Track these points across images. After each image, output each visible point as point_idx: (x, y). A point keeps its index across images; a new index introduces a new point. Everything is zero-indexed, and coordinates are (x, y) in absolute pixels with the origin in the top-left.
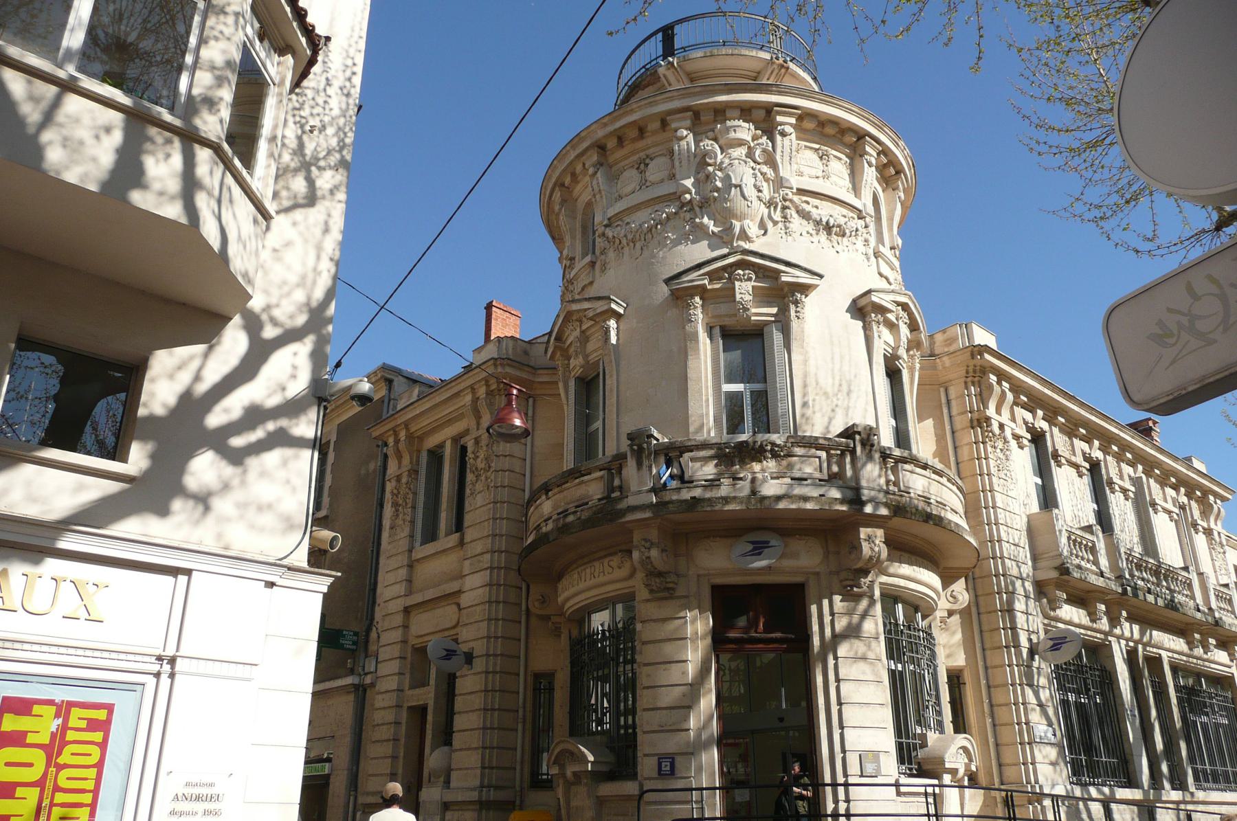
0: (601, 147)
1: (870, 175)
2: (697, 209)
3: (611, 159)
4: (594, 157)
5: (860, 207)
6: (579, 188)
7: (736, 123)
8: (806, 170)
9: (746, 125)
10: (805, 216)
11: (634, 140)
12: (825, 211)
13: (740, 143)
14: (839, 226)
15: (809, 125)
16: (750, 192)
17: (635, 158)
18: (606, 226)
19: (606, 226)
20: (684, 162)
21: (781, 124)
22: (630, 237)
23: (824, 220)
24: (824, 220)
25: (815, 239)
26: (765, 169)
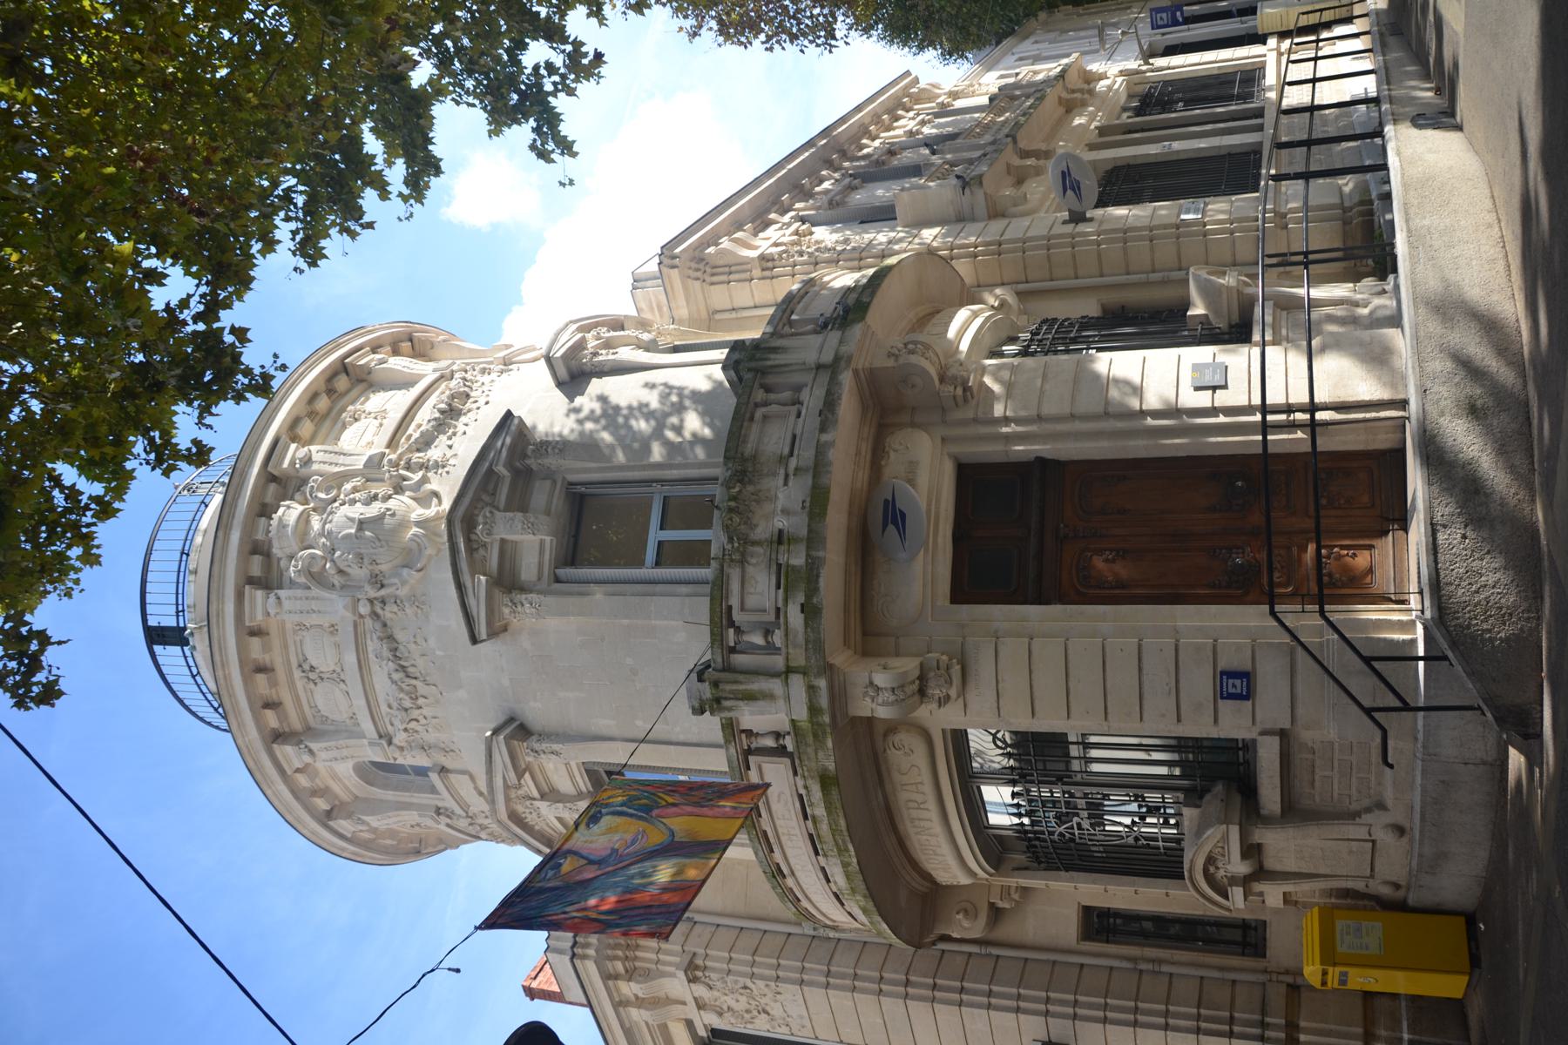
0: (278, 737)
1: (398, 363)
2: (383, 592)
3: (297, 725)
4: (287, 752)
5: (437, 375)
6: (336, 788)
7: (274, 523)
8: (368, 438)
9: (281, 510)
10: (426, 442)
11: (273, 684)
12: (426, 415)
13: (304, 519)
14: (452, 397)
15: (306, 428)
16: (375, 509)
17: (300, 684)
18: (390, 743)
19: (390, 743)
20: (314, 605)
21: (293, 463)
22: (407, 703)
23: (437, 415)
24: (437, 415)
25: (461, 428)
26: (348, 486)
